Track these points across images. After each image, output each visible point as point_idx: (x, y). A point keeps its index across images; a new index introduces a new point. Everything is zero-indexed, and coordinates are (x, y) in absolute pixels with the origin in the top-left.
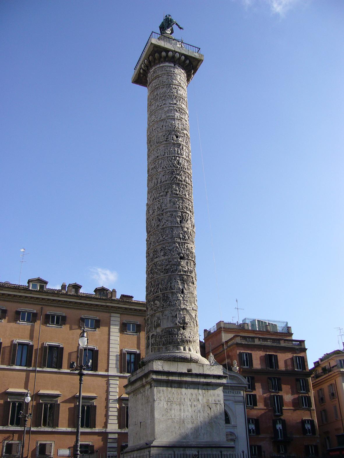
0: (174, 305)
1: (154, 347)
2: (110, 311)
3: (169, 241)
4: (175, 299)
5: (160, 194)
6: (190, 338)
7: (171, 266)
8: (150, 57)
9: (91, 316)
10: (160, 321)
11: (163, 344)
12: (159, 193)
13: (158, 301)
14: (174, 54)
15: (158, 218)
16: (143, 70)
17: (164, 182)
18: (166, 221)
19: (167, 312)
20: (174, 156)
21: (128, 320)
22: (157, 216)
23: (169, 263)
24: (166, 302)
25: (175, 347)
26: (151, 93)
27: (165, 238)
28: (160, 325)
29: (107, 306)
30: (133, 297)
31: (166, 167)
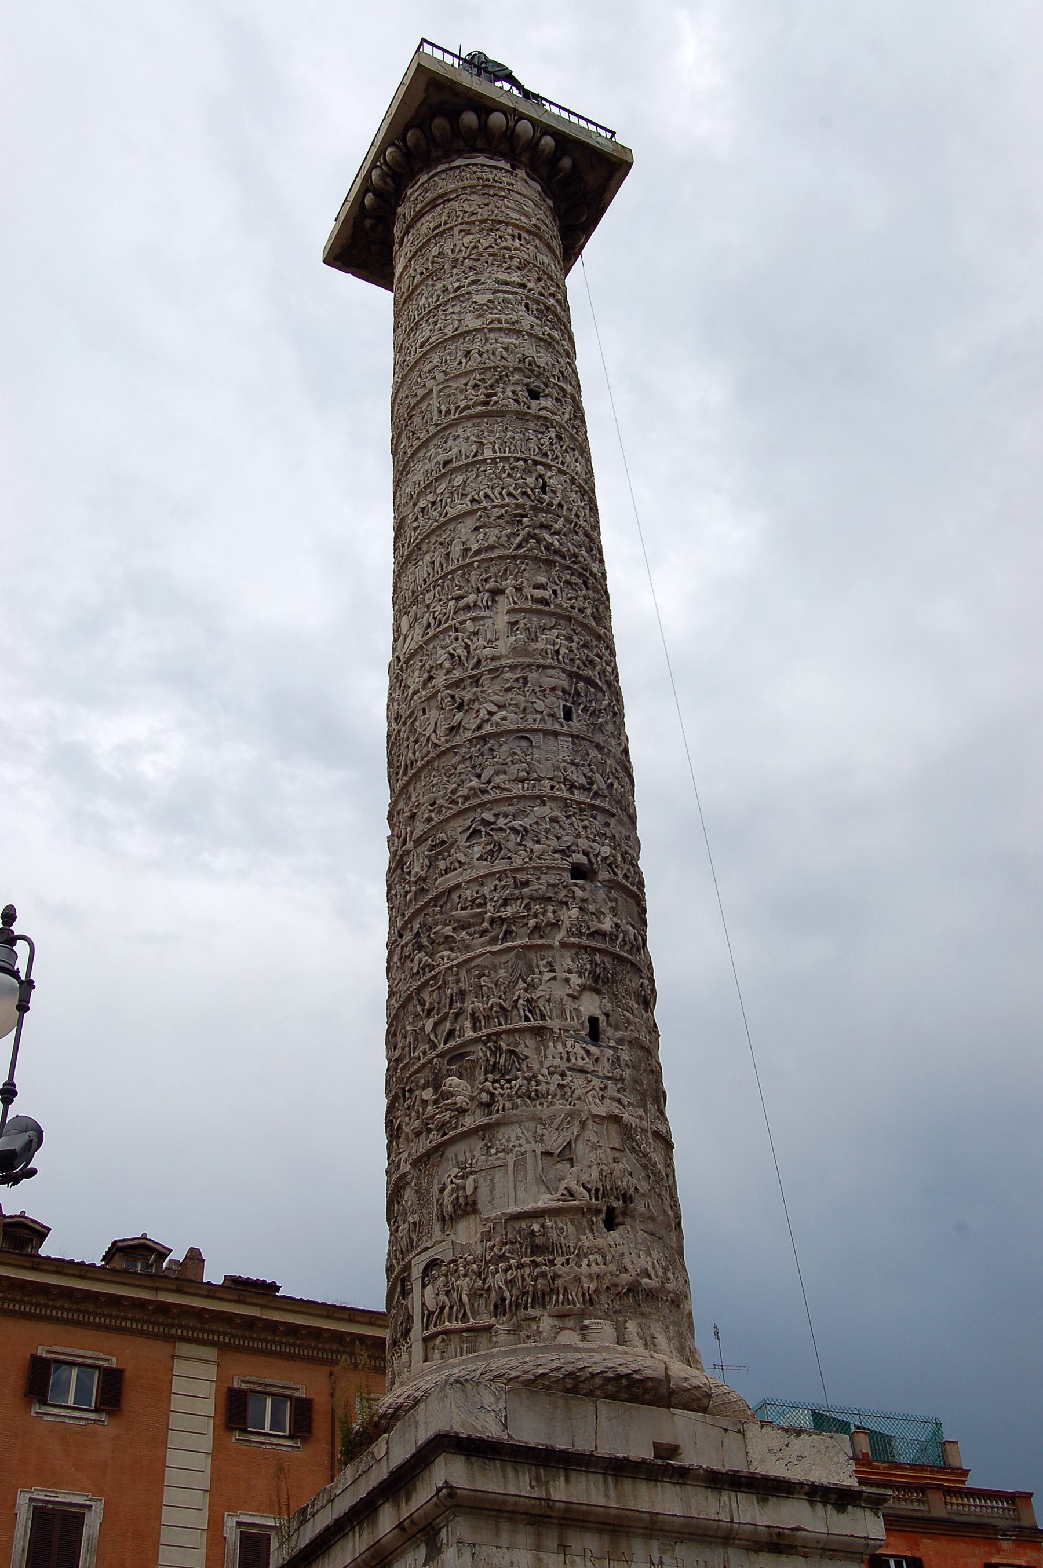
0: (554, 1096)
1: (440, 1328)
2: (173, 1331)
3: (514, 791)
4: (556, 1067)
5: (462, 603)
6: (649, 1277)
7: (527, 907)
8: (409, 134)
9: (84, 1353)
10: (475, 1181)
11: (496, 1307)
12: (458, 598)
13: (460, 1078)
14: (511, 124)
15: (453, 697)
16: (378, 194)
17: (478, 552)
18: (493, 708)
19: (510, 1135)
20: (525, 460)
21: (254, 1379)
22: (447, 687)
23: (517, 892)
24: (509, 1081)
25: (570, 1323)
26: (410, 261)
27: (489, 782)
28: (475, 1203)
29: (165, 1308)
30: (278, 1289)
31: (486, 496)
